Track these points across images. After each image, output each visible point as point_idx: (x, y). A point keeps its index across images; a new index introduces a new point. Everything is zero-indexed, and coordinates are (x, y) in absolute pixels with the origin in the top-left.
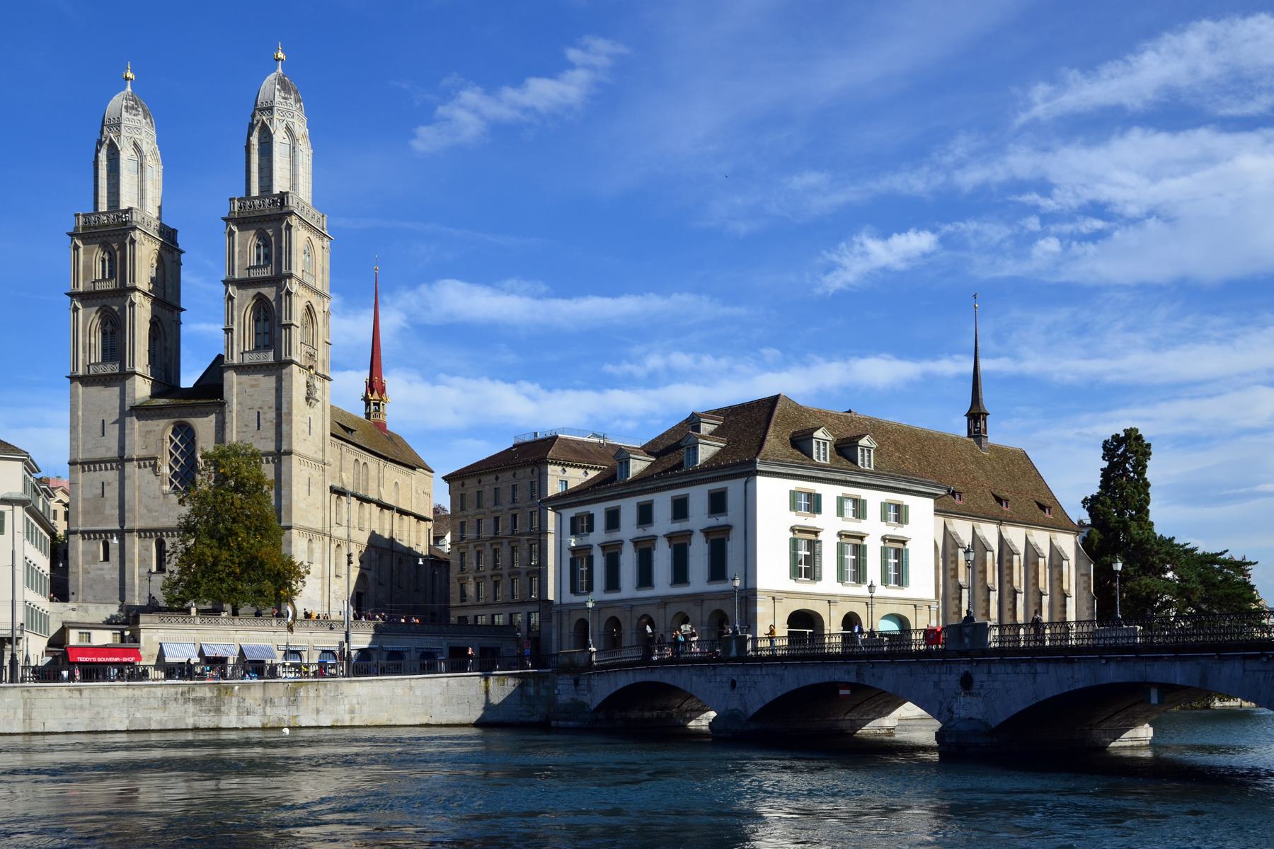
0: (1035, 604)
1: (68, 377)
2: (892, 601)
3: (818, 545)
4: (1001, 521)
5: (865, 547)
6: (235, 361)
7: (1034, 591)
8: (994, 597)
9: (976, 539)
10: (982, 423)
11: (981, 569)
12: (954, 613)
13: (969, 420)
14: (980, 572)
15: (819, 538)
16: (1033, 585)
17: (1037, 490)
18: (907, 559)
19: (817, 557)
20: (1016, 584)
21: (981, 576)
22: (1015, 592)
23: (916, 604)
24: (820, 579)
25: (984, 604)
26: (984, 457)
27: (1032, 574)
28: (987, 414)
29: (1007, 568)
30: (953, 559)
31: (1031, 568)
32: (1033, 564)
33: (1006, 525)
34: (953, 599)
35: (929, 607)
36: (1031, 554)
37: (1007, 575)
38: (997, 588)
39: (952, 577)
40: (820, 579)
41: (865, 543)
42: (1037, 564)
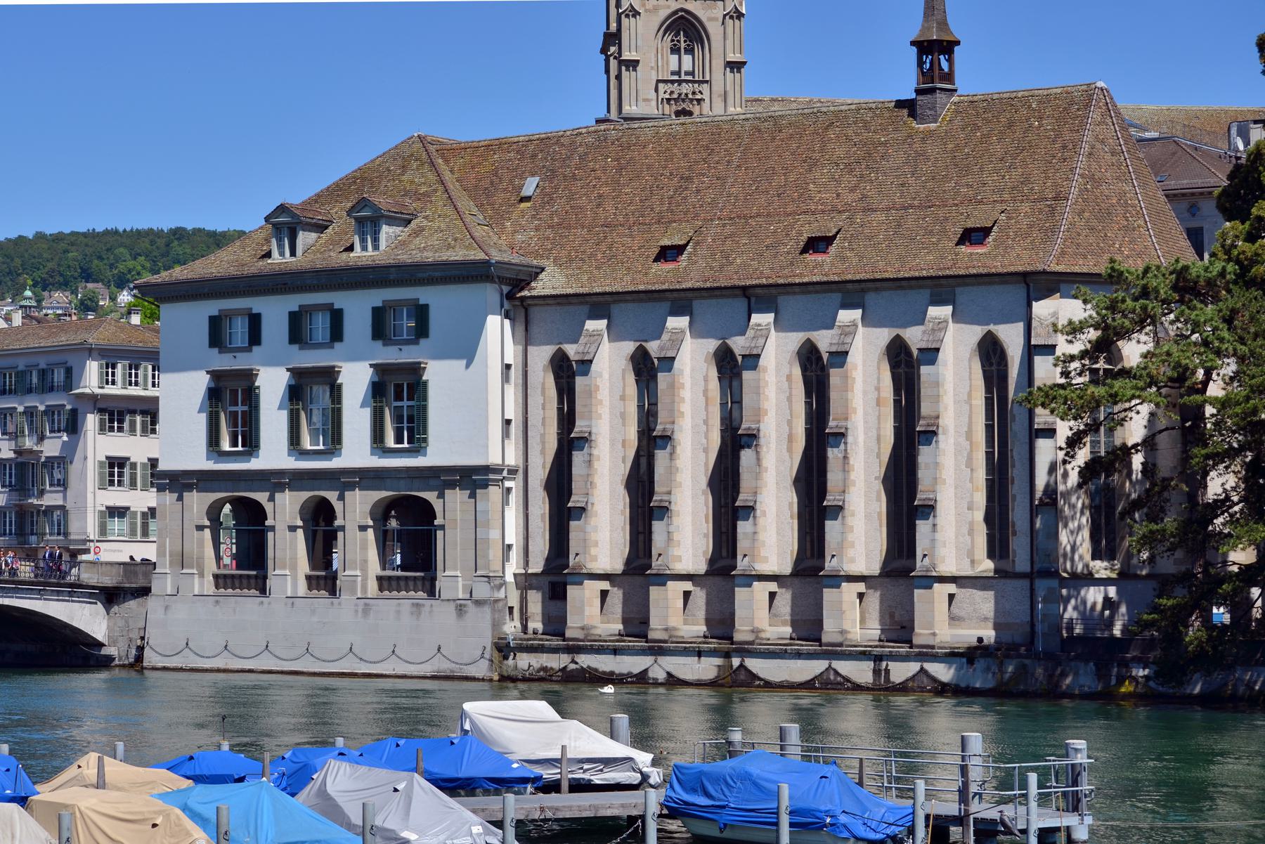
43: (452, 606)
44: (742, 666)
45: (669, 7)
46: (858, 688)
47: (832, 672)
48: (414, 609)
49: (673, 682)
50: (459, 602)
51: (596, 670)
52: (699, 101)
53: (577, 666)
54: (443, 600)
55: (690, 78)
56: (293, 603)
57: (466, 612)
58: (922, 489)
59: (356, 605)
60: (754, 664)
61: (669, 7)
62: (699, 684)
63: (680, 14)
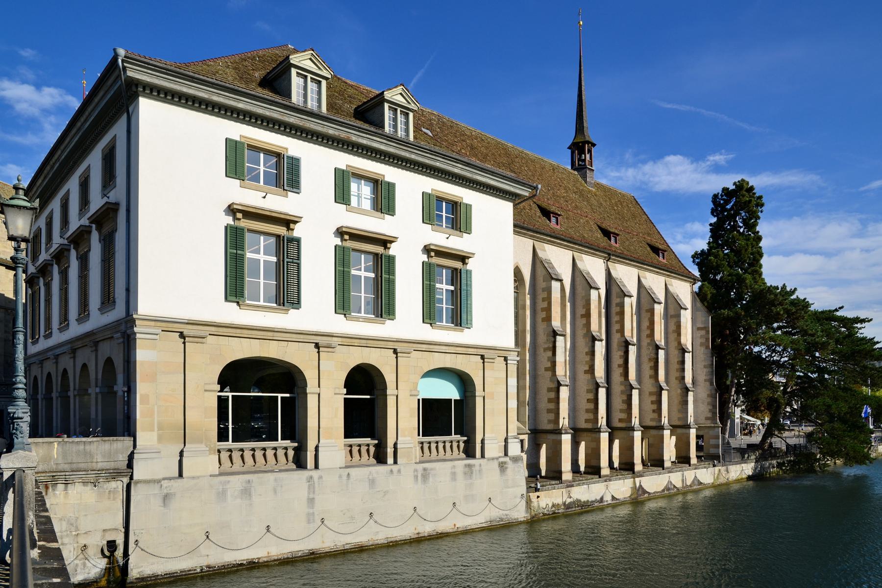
0: (650, 360)
3: (293, 246)
5: (391, 260)
7: (649, 344)
8: (600, 348)
9: (577, 273)
10: (588, 156)
11: (583, 312)
12: (546, 369)
13: (573, 153)
14: (582, 316)
16: (648, 336)
17: (649, 234)
18: (469, 285)
20: (627, 334)
21: (584, 321)
22: (627, 344)
25: (588, 358)
26: (590, 191)
27: (645, 324)
29: (617, 314)
30: (545, 295)
31: (645, 316)
32: (647, 311)
33: (615, 262)
34: (545, 350)
35: (506, 359)
36: (645, 300)
37: (617, 322)
38: (604, 337)
39: (543, 320)
41: (391, 252)
42: (652, 312)
56: (349, 474)
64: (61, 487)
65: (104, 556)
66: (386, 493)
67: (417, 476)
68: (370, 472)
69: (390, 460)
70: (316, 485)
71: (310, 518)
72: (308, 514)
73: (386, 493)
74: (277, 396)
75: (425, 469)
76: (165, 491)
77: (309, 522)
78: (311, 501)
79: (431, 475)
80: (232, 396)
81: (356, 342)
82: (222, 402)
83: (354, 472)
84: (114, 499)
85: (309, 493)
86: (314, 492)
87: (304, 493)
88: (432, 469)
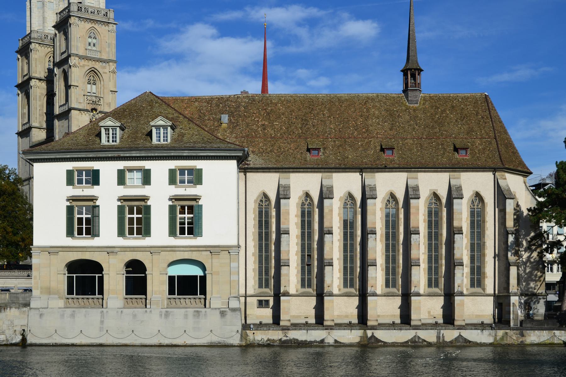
1: (16, 134)
2: (182, 249)
4: (361, 170)
6: (57, 113)
15: (97, 204)
19: (97, 218)
23: (213, 250)
24: (98, 236)
28: (420, 70)
40: (98, 236)
43: (218, 312)
44: (373, 336)
45: (89, 66)
46: (430, 345)
47: (417, 338)
48: (196, 313)
49: (338, 344)
50: (222, 309)
51: (297, 340)
52: (99, 105)
53: (288, 338)
54: (212, 309)
55: (95, 95)
56: (122, 311)
57: (226, 314)
58: (456, 258)
59: (161, 312)
60: (381, 335)
61: (89, 66)
62: (351, 345)
63: (93, 69)
64: (9, 309)
65: (21, 335)
66: (142, 321)
67: (162, 315)
68: (134, 311)
69: (148, 306)
70: (105, 315)
71: (101, 329)
72: (100, 327)
73: (142, 321)
74: (96, 276)
75: (167, 312)
76: (41, 313)
77: (100, 331)
78: (102, 322)
79: (170, 315)
80: (76, 276)
81: (128, 249)
82: (70, 279)
83: (125, 311)
84: (25, 314)
85: (101, 318)
86: (104, 318)
87: (98, 318)
88: (171, 312)
